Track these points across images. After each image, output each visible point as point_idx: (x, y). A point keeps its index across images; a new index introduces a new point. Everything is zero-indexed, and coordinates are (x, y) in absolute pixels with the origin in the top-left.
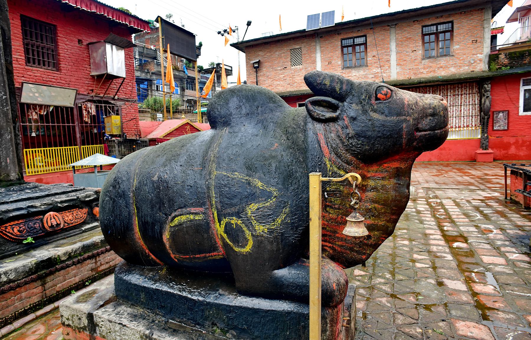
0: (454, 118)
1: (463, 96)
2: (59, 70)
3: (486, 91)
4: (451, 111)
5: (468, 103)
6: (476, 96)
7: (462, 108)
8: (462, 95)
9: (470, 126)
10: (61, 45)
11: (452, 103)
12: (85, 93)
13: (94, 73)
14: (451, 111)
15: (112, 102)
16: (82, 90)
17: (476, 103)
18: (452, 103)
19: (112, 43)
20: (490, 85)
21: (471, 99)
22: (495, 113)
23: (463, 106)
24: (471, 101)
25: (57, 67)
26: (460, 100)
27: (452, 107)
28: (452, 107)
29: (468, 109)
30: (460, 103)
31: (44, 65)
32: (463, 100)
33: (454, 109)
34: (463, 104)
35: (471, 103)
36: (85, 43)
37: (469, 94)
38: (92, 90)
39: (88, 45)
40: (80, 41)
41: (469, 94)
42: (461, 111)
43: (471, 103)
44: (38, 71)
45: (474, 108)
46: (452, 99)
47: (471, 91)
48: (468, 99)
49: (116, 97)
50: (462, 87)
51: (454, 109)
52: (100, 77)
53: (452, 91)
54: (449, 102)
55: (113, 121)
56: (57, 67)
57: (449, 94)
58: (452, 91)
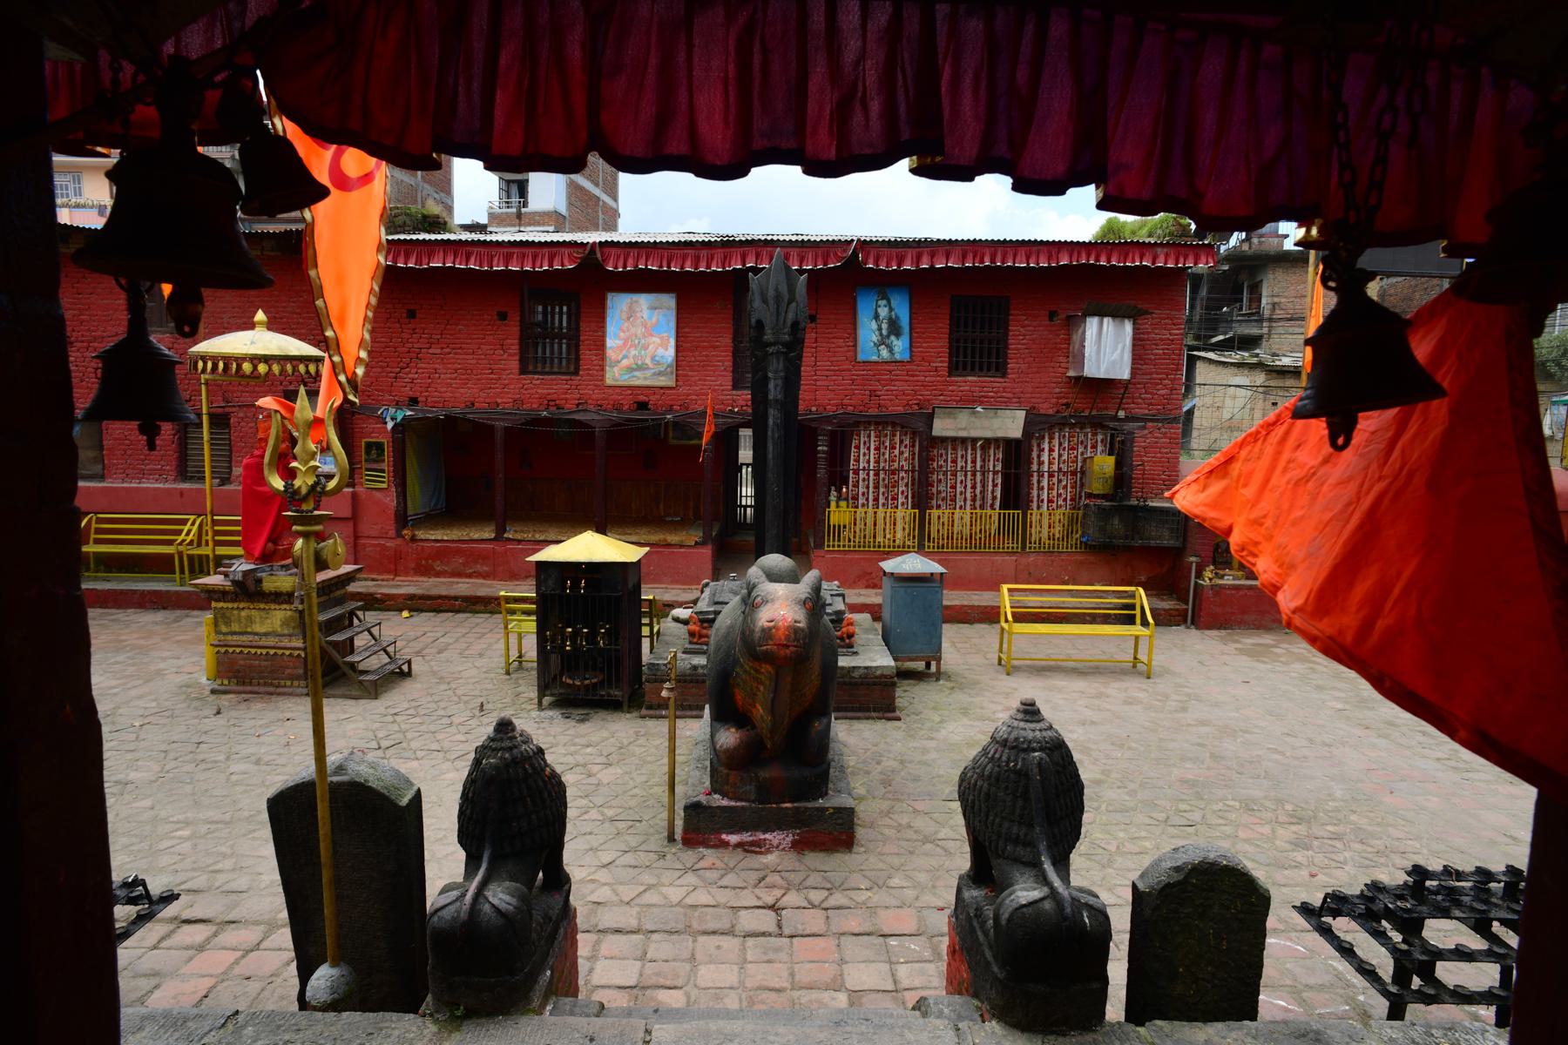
2: (1004, 375)
10: (1014, 329)
12: (1051, 412)
13: (1071, 373)
15: (1111, 424)
16: (1045, 405)
19: (1101, 314)
25: (1000, 369)
31: (981, 369)
36: (1063, 316)
38: (1067, 405)
39: (1069, 318)
40: (1052, 316)
44: (969, 382)
49: (1121, 414)
52: (1078, 379)
55: (1096, 468)
56: (1000, 369)
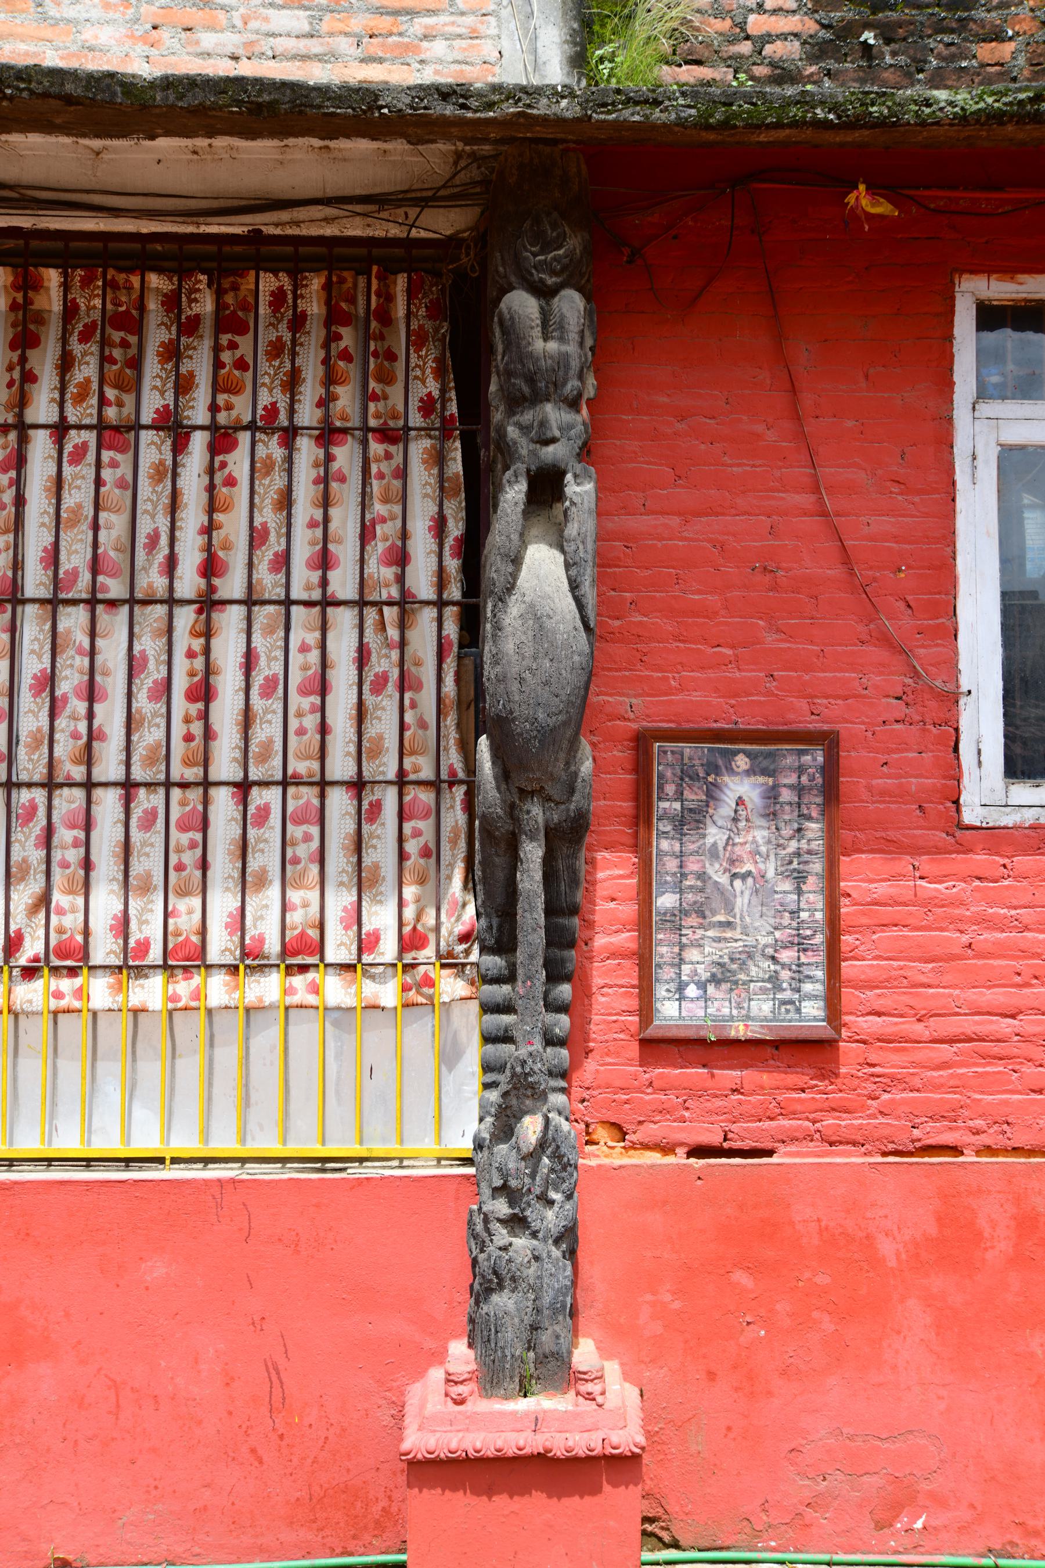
0: (108, 804)
1: (238, 462)
3: (535, 387)
4: (70, 682)
5: (303, 580)
6: (421, 478)
7: (228, 649)
8: (221, 441)
9: (339, 947)
11: (75, 557)
14: (70, 682)
17: (423, 586)
18: (75, 557)
20: (571, 304)
21: (345, 521)
22: (665, 759)
23: (231, 620)
24: (346, 551)
26: (192, 517)
27: (73, 621)
28: (73, 621)
29: (302, 665)
30: (190, 558)
32: (234, 526)
33: (113, 652)
34: (232, 585)
35: (343, 583)
37: (328, 435)
41: (328, 435)
42: (203, 692)
43: (343, 583)
45: (384, 663)
46: (78, 496)
47: (346, 398)
48: (304, 509)
50: (230, 323)
51: (113, 652)
53: (87, 370)
54: (37, 538)
57: (42, 408)
58: (87, 370)
